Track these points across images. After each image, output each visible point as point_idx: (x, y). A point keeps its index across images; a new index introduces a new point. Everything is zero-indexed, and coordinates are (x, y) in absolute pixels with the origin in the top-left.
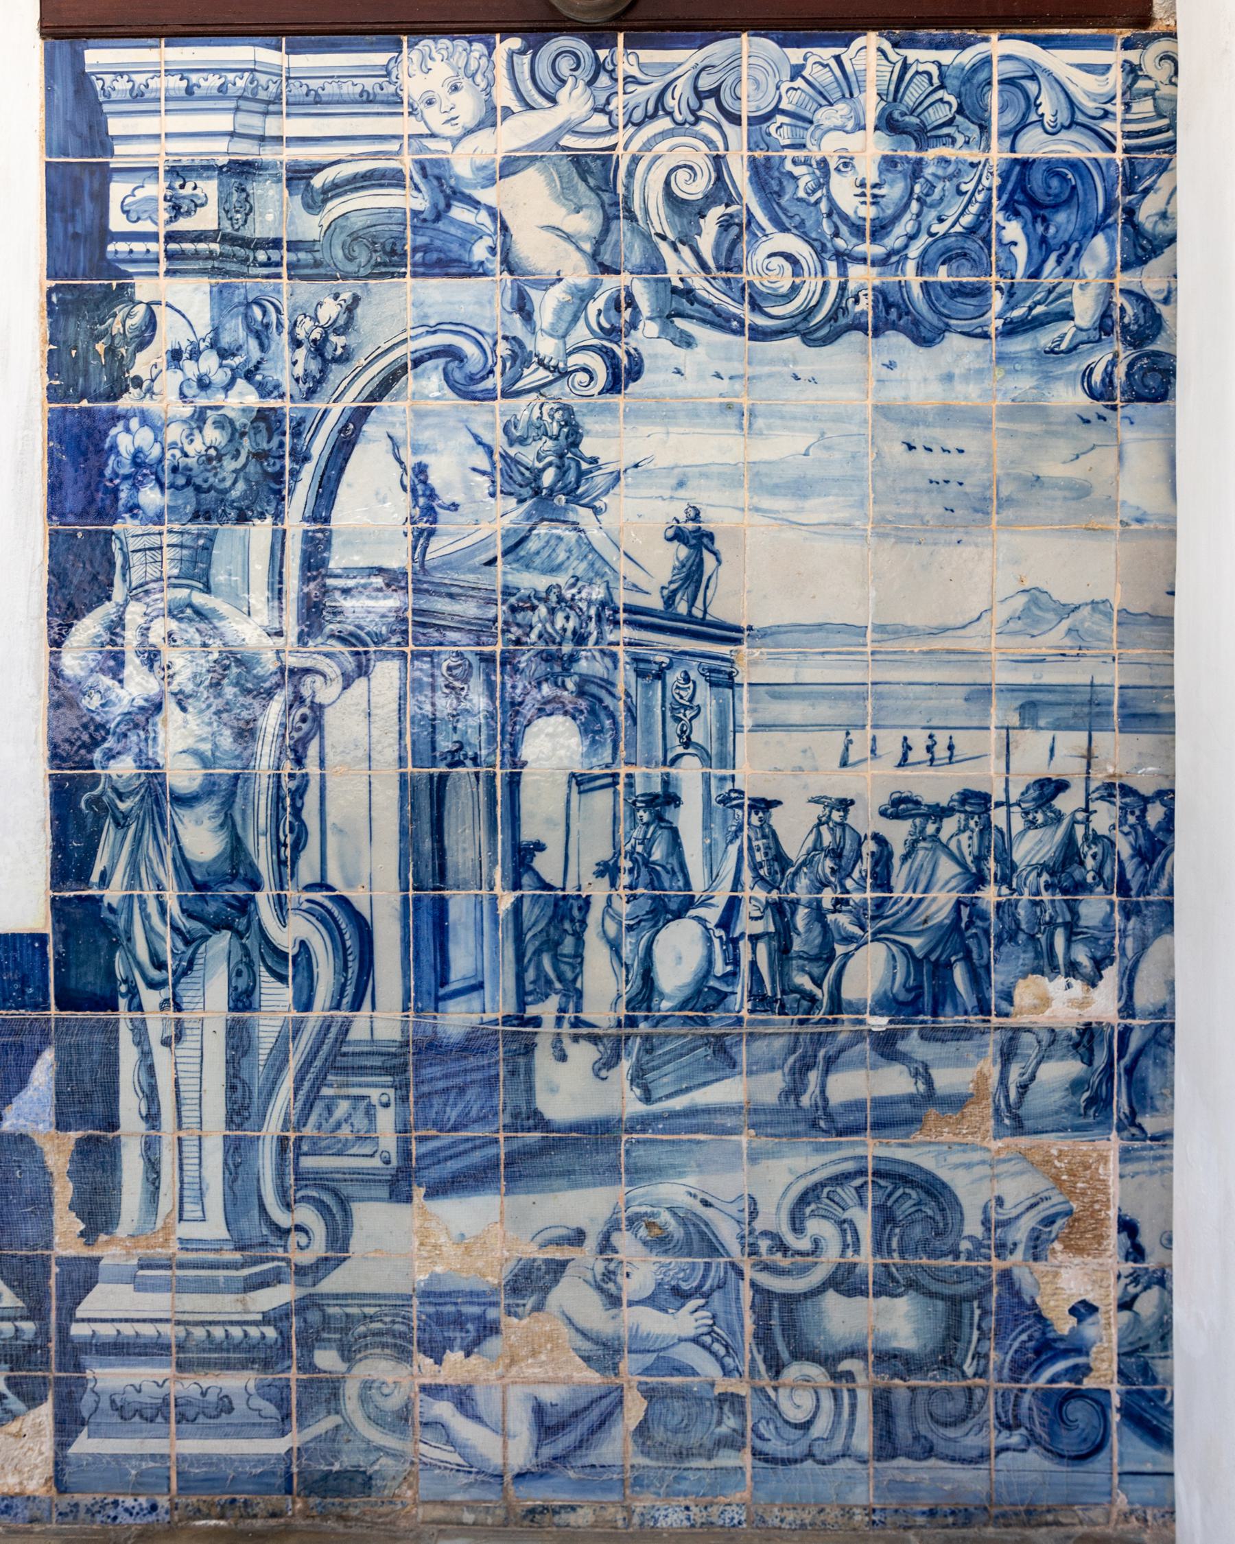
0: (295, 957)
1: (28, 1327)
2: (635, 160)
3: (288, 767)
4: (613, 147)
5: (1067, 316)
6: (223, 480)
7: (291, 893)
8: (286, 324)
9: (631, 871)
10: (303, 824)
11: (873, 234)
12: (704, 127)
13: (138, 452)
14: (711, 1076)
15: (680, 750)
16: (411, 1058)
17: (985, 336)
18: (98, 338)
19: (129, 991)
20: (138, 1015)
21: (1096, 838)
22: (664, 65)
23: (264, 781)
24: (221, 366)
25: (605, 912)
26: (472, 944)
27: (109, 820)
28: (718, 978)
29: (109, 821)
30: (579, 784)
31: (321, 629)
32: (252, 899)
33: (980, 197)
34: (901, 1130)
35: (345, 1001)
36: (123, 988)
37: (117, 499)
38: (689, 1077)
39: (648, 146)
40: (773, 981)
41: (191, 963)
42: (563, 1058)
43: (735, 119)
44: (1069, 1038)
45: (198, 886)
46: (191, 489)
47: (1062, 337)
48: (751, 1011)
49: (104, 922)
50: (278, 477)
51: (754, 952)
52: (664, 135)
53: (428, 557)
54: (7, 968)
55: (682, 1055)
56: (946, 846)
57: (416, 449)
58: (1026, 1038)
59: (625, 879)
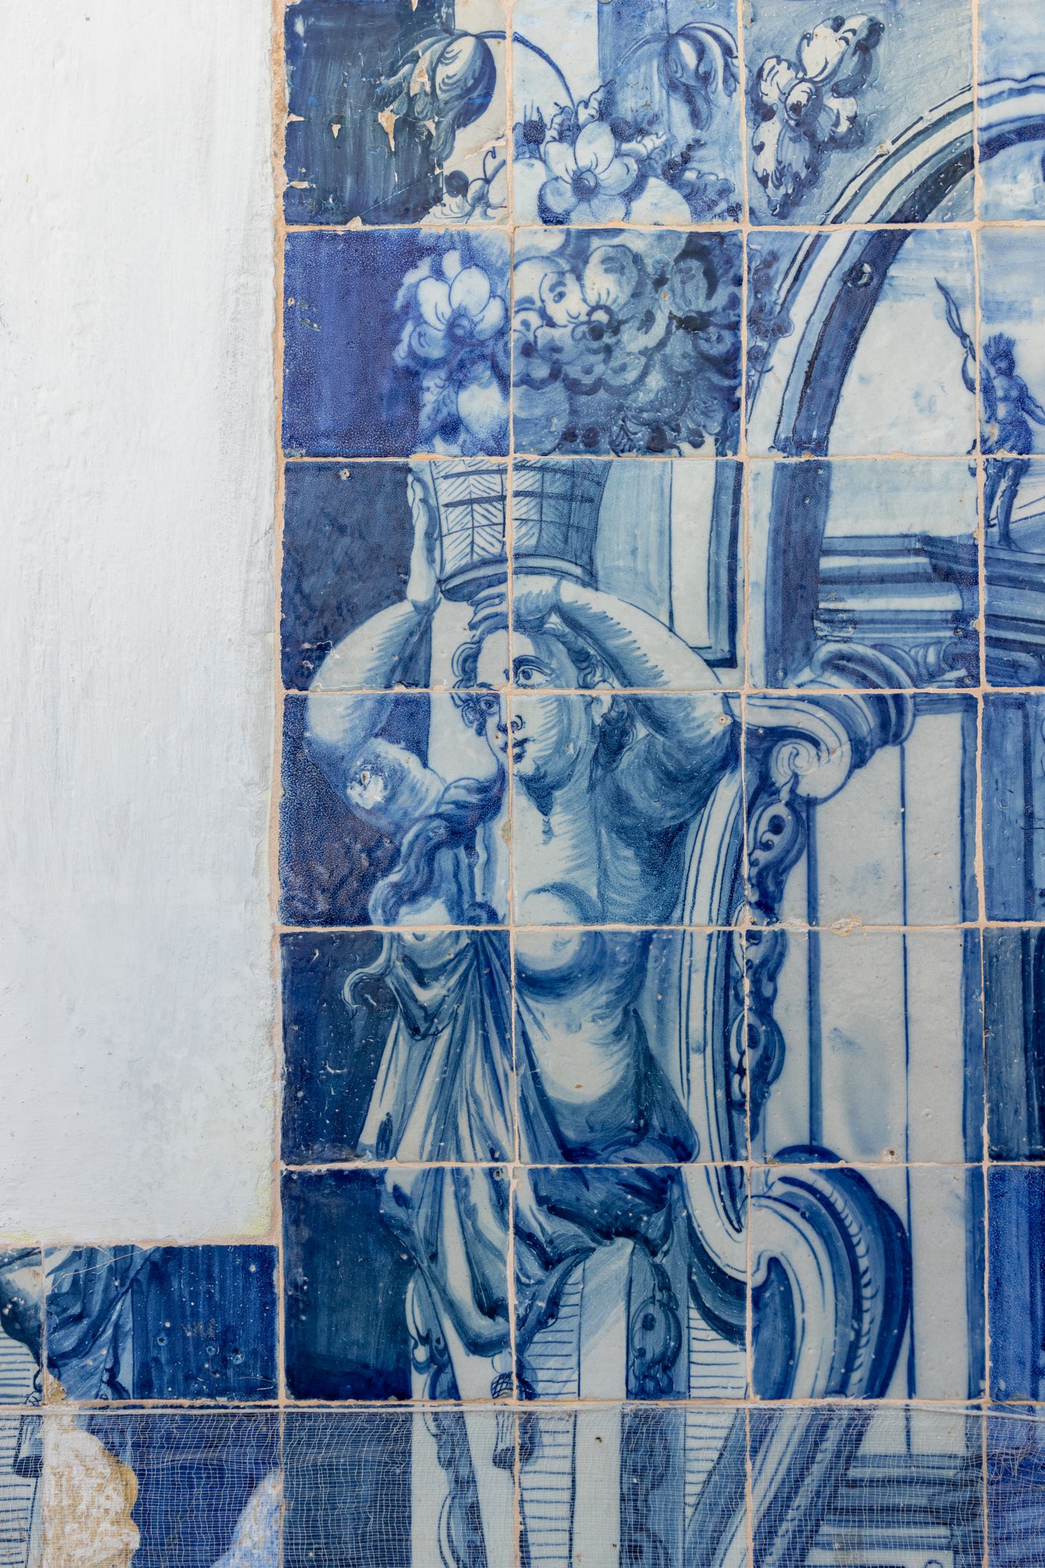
0: (758, 1291)
3: (746, 919)
6: (623, 368)
8: (743, 74)
10: (774, 1029)
16: (984, 1492)
18: (383, 102)
19: (432, 1359)
20: (448, 1406)
23: (700, 946)
24: (618, 154)
27: (397, 1025)
29: (397, 1025)
31: (808, 653)
32: (675, 1177)
35: (855, 1377)
36: (421, 1354)
37: (415, 406)
41: (554, 1302)
45: (569, 1153)
49: (385, 1222)
50: (727, 364)
53: (1016, 515)
57: (992, 310)
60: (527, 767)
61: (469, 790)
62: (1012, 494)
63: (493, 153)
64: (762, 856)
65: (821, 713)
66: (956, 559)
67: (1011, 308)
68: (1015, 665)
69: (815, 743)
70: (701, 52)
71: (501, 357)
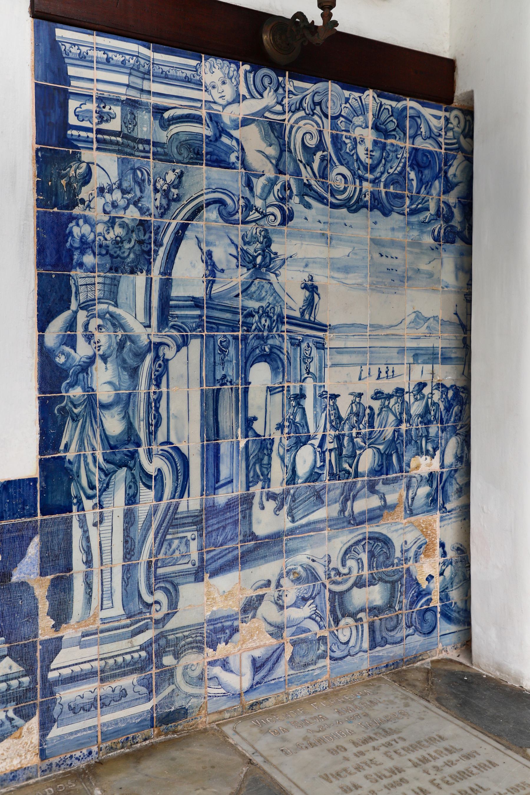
0: (155, 477)
1: (26, 680)
2: (292, 127)
3: (153, 388)
4: (284, 120)
5: (427, 209)
6: (124, 252)
7: (154, 447)
8: (152, 181)
9: (289, 426)
10: (159, 415)
11: (370, 171)
12: (316, 118)
13: (83, 236)
14: (315, 508)
15: (306, 375)
16: (204, 517)
17: (403, 214)
18: (63, 177)
19: (78, 502)
20: (82, 513)
21: (434, 404)
22: (302, 88)
23: (143, 395)
24: (122, 198)
25: (279, 445)
26: (229, 463)
27: (69, 418)
28: (318, 468)
29: (69, 418)
30: (270, 391)
31: (167, 324)
32: (137, 451)
33: (403, 160)
34: (376, 521)
35: (177, 494)
36: (75, 501)
37: (72, 259)
38: (308, 509)
39: (296, 122)
40: (336, 467)
41: (108, 485)
42: (263, 508)
43: (326, 116)
44: (426, 478)
45: (112, 448)
46: (108, 256)
47: (427, 217)
48: (329, 480)
49: (66, 469)
50: (149, 253)
51: (330, 456)
52: (302, 118)
53: (212, 292)
54: (16, 497)
55: (305, 501)
56: (391, 410)
57: (208, 244)
58: (414, 480)
59: (286, 430)
60: (101, 352)
61: (87, 358)
62: (211, 288)
63: (91, 194)
64: (157, 373)
65: (170, 339)
66: (200, 302)
67: (212, 243)
68: (212, 327)
69: (169, 346)
70: (142, 174)
71: (94, 247)
